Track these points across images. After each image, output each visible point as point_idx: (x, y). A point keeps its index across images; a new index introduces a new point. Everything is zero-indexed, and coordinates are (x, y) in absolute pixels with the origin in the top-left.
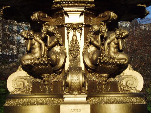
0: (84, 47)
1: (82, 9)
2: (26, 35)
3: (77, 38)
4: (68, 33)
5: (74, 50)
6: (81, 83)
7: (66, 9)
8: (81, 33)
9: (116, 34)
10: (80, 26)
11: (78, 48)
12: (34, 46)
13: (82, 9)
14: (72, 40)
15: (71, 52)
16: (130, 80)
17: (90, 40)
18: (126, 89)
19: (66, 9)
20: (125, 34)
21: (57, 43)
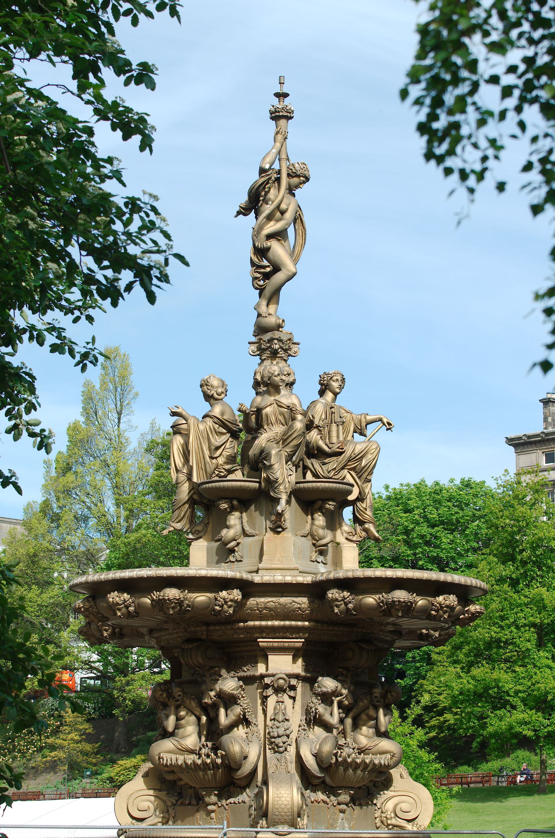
0: (300, 726)
1: (298, 642)
2: (165, 695)
3: (285, 708)
4: (265, 699)
5: (279, 736)
6: (296, 810)
7: (263, 642)
8: (294, 698)
9: (371, 693)
10: (293, 682)
11: (288, 732)
12: (183, 722)
13: (298, 642)
14: (275, 714)
15: (273, 740)
16: (403, 802)
17: (316, 713)
18: (393, 821)
19: (263, 642)
20: (393, 696)
21: (244, 721)
